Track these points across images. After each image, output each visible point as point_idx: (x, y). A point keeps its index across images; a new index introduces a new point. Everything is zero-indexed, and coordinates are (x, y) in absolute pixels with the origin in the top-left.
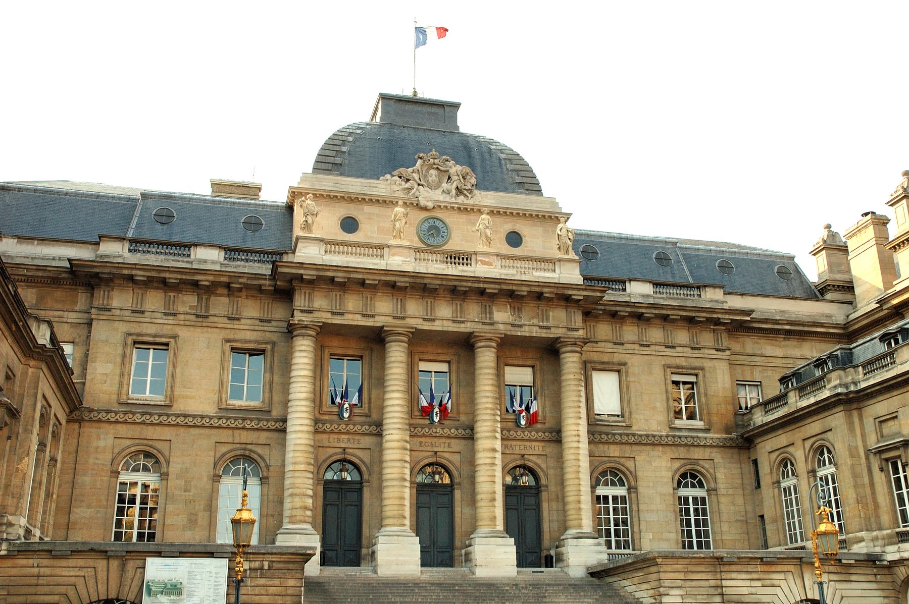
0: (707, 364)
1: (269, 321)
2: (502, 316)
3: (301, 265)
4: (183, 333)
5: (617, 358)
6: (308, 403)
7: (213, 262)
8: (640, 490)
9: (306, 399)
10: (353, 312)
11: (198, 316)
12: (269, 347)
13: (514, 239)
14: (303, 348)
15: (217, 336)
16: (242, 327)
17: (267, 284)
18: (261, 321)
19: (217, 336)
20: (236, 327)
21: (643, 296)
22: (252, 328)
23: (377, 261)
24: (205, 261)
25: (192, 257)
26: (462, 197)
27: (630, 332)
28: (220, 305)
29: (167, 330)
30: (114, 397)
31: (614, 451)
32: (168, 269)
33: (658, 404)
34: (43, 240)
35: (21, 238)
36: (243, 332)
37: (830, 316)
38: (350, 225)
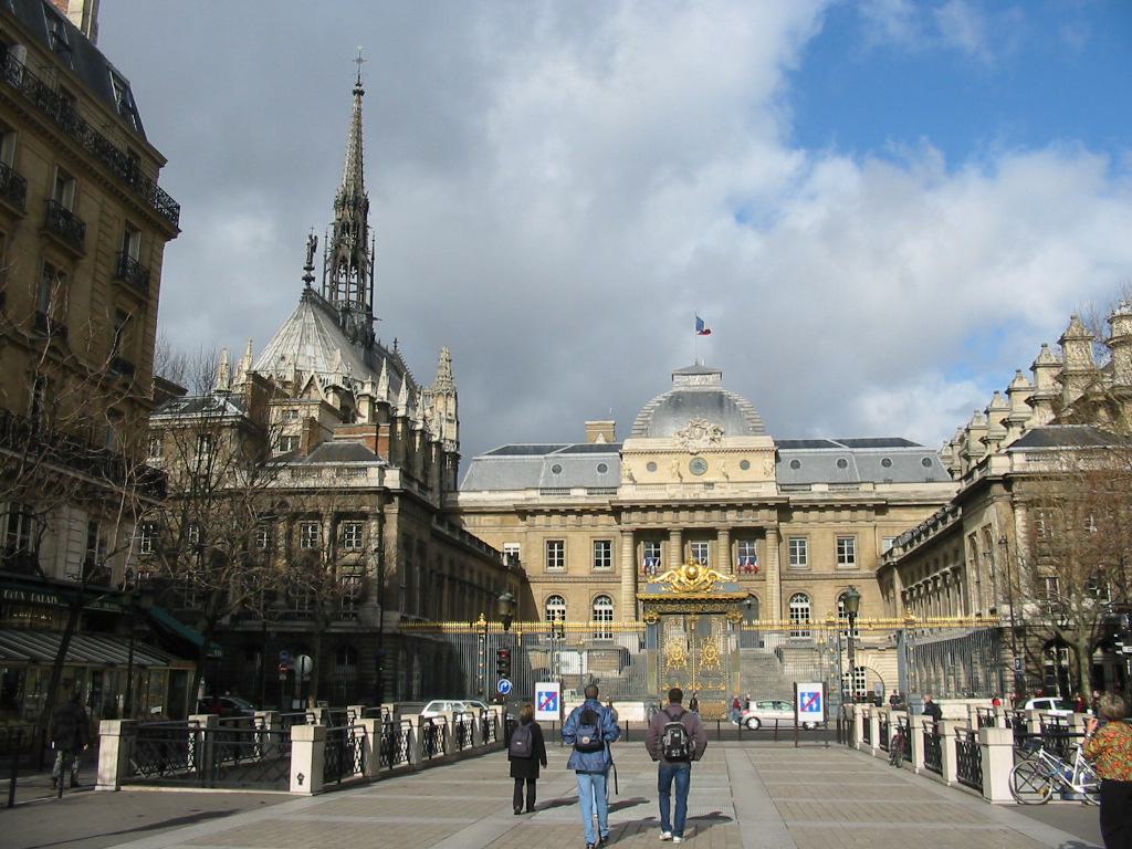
0: (861, 530)
2: (731, 516)
3: (622, 501)
4: (570, 535)
5: (804, 531)
7: (582, 497)
8: (815, 605)
10: (651, 521)
13: (745, 465)
15: (586, 535)
19: (586, 535)
21: (823, 493)
23: (663, 492)
24: (576, 497)
26: (713, 445)
27: (813, 515)
28: (587, 518)
29: (562, 534)
30: (541, 570)
31: (801, 584)
33: (828, 556)
34: (500, 491)
35: (490, 491)
37: (949, 492)
38: (652, 467)
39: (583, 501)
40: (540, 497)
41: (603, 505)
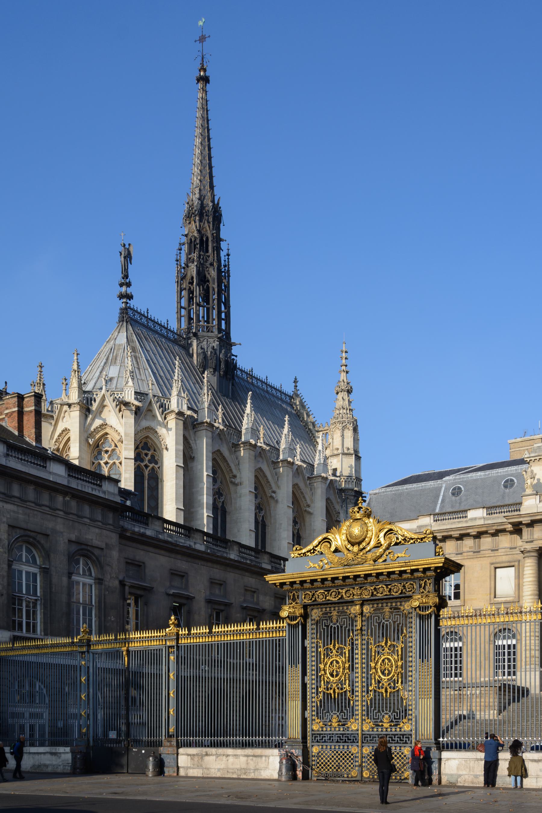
1: (515, 548)
6: (532, 597)
7: (480, 518)
9: (531, 595)
11: (474, 552)
12: (516, 564)
14: (528, 564)
16: (499, 554)
17: (509, 527)
18: (511, 548)
20: (496, 554)
22: (506, 554)
24: (475, 519)
25: (469, 517)
32: (452, 530)
36: (500, 557)
39: (481, 522)
40: (434, 524)
41: (502, 523)
